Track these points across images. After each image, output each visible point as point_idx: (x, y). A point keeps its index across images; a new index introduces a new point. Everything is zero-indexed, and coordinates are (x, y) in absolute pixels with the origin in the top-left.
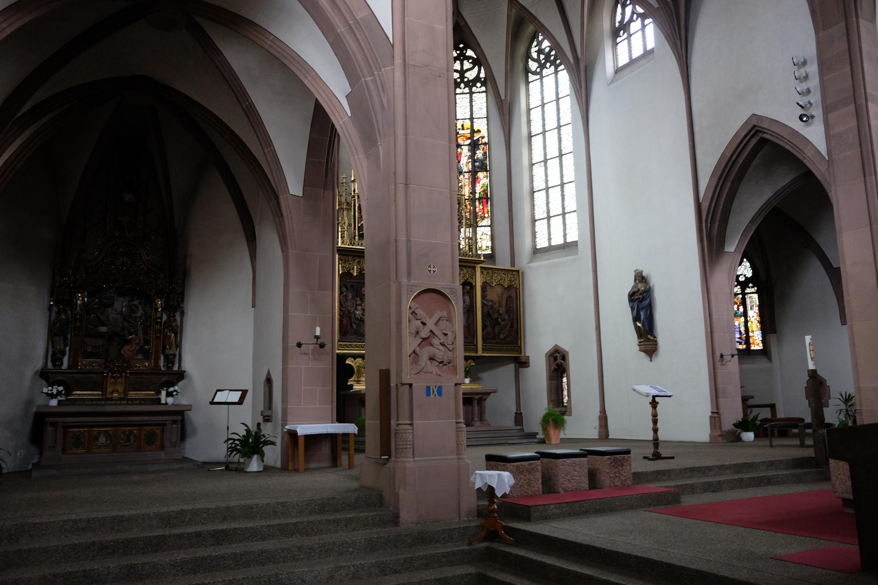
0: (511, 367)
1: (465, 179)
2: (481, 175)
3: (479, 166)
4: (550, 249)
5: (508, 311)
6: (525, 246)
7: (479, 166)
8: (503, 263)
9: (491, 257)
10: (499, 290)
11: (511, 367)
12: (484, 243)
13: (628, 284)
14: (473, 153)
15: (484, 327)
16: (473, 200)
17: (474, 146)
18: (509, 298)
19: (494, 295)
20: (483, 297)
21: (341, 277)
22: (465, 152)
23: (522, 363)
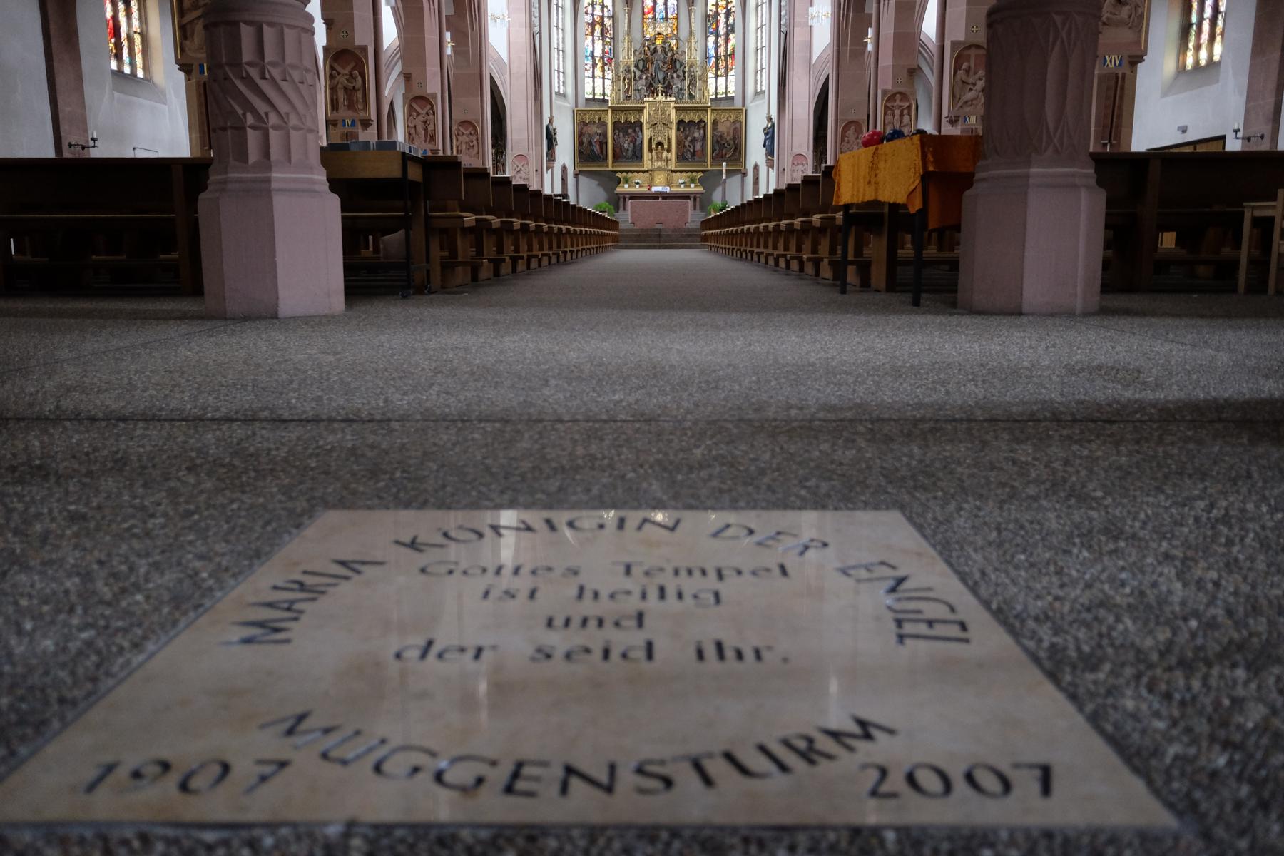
0: (739, 176)
1: (721, 41)
2: (731, 36)
3: (730, 29)
4: (762, 92)
5: (734, 138)
6: (750, 89)
7: (730, 29)
8: (738, 105)
9: (732, 98)
10: (728, 124)
11: (739, 176)
12: (731, 88)
13: (765, 124)
14: (727, 18)
15: (713, 150)
16: (726, 56)
17: (728, 14)
18: (735, 129)
19: (722, 128)
20: (714, 129)
21: (616, 124)
22: (722, 19)
23: (744, 174)
